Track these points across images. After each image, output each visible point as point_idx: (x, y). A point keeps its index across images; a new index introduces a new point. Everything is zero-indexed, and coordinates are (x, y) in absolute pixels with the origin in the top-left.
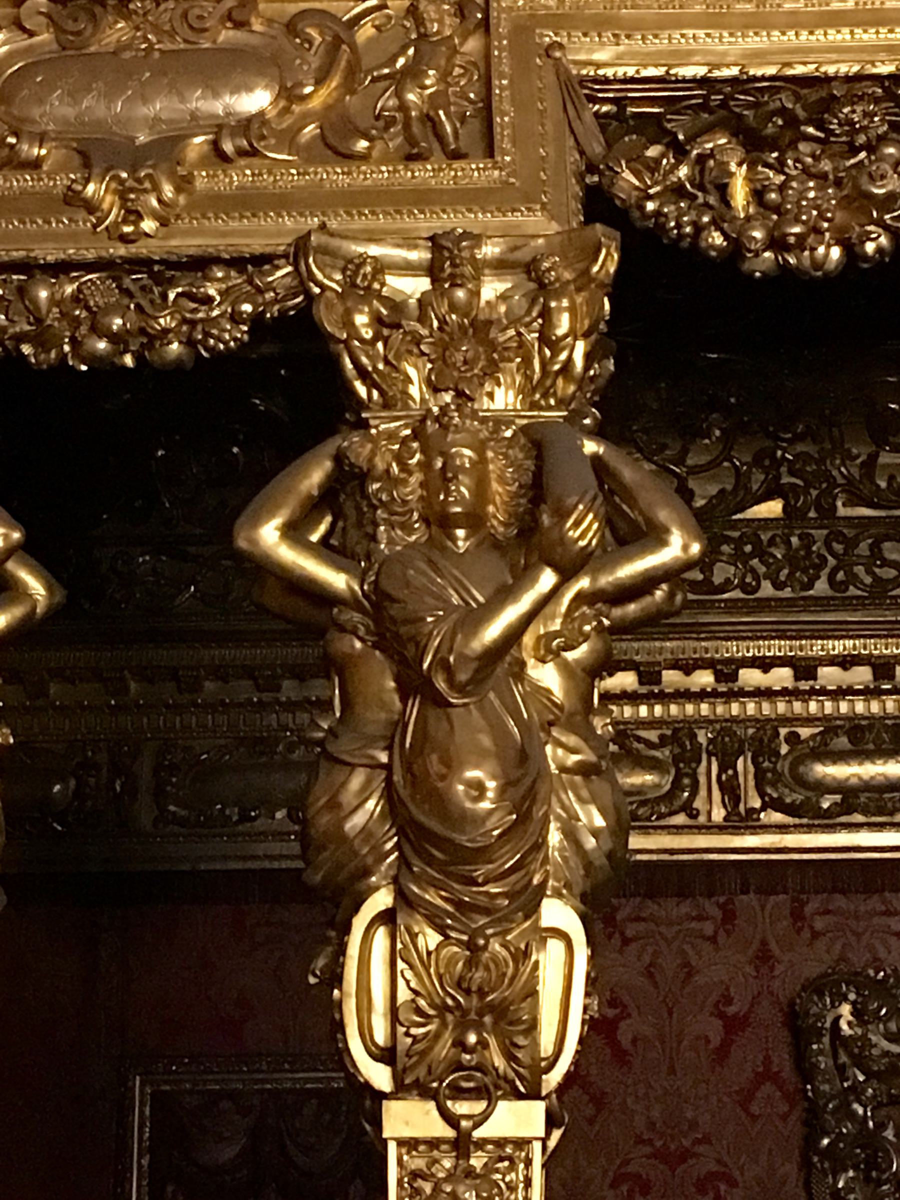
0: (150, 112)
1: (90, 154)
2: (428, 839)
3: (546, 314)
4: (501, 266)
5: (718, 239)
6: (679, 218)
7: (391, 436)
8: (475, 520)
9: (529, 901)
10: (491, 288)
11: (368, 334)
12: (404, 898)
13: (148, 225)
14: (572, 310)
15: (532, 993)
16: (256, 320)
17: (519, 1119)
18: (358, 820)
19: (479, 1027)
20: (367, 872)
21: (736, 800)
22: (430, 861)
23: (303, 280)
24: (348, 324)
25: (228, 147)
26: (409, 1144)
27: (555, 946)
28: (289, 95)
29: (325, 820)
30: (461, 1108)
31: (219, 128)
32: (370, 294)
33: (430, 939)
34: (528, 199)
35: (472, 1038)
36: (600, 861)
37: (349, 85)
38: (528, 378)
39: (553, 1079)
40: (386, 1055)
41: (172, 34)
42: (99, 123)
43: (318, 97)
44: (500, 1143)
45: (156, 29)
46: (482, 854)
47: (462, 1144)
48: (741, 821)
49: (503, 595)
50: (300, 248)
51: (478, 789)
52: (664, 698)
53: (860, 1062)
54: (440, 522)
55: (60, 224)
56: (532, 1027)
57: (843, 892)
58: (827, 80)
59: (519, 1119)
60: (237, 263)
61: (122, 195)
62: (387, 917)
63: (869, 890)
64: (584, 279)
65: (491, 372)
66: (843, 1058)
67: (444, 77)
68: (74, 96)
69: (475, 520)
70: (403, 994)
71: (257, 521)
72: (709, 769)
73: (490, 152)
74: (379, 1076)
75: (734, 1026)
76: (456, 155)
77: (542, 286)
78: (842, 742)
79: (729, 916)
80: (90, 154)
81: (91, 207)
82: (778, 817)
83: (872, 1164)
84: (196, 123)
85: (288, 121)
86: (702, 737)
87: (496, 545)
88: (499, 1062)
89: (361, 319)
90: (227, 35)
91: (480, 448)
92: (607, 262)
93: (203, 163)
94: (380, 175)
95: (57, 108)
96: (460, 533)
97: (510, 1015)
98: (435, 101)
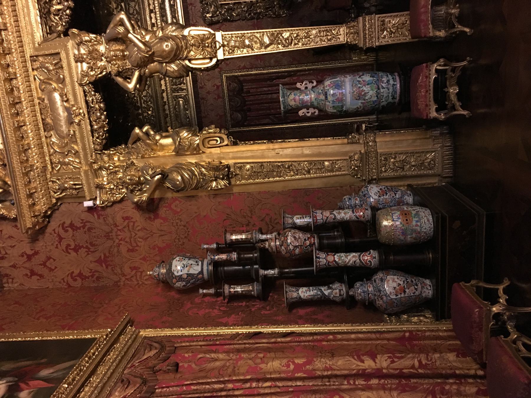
1: (70, 122)
3: (86, 41)
4: (79, 50)
5: (68, 12)
6: (65, 19)
7: (111, 67)
9: (184, 37)
10: (83, 51)
11: (94, 72)
12: (186, 58)
13: (81, 111)
14: (84, 37)
15: (199, 35)
16: (95, 92)
17: (219, 35)
18: (176, 68)
19: (205, 44)
20: (183, 65)
22: (180, 54)
23: (86, 84)
24: (93, 76)
25: (65, 99)
26: (224, 54)
28: (55, 90)
29: (176, 74)
30: (218, 47)
31: (63, 101)
32: (87, 72)
33: (192, 53)
34: (66, 46)
35: (207, 45)
37: (51, 79)
38: (97, 44)
39: (212, 32)
40: (211, 59)
41: (47, 111)
42: (66, 122)
43: (54, 85)
44: (223, 39)
45: (47, 114)
46: (177, 45)
47: (223, 46)
49: (135, 45)
50: (81, 85)
51: (167, 46)
53: (216, 13)
54: (124, 57)
56: (204, 35)
57: (189, 17)
59: (219, 35)
60: (86, 96)
61: (77, 116)
62: (190, 61)
64: (79, 35)
65: (97, 50)
66: (215, 15)
67: (47, 63)
69: (123, 51)
70: (201, 57)
71: (128, 88)
73: (58, 54)
74: (214, 61)
76: (60, 59)
77: (81, 43)
78: (164, 18)
81: (80, 121)
83: (231, 9)
84: (63, 105)
85: (59, 89)
87: (127, 48)
88: (210, 40)
89: (92, 73)
90: (46, 101)
91: (110, 51)
92: (75, 31)
93: (69, 103)
94: (66, 73)
95: (64, 128)
96: (125, 53)
97: (203, 39)
98: (52, 64)
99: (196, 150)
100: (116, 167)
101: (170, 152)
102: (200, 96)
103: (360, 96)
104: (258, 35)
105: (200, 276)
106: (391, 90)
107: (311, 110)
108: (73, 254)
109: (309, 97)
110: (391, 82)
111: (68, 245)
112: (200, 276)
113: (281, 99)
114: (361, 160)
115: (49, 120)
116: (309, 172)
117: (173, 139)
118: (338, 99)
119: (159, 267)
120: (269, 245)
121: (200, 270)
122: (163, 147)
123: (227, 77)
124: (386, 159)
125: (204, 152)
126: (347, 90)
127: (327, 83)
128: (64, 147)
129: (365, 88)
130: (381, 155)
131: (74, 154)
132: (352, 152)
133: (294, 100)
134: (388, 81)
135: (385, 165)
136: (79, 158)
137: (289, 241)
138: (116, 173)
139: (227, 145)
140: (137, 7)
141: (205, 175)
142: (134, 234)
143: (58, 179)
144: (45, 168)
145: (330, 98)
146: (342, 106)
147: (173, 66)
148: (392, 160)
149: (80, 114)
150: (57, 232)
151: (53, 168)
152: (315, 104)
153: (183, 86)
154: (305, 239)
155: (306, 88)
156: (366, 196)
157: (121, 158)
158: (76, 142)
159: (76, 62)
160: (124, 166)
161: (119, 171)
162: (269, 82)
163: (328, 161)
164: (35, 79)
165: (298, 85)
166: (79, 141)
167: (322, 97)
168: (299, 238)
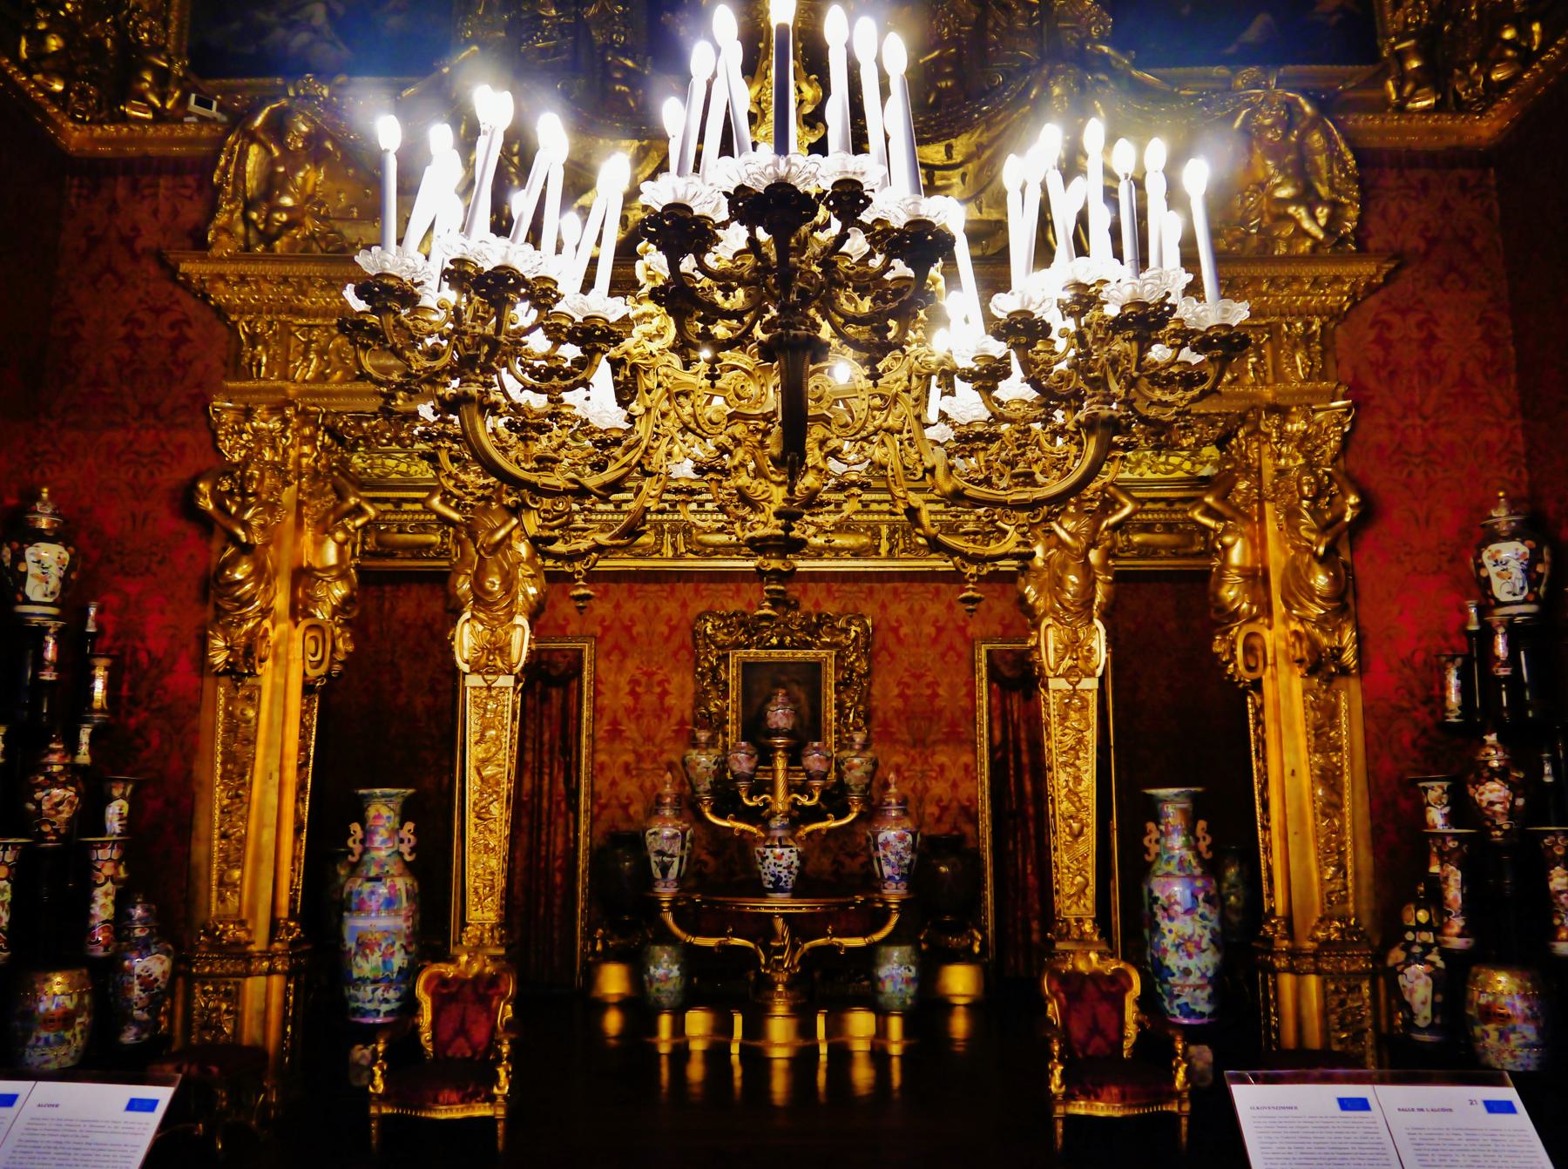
2: (482, 599)
12: (473, 616)
15: (509, 644)
21: (675, 549)
30: (488, 677)
33: (480, 628)
39: (517, 670)
40: (467, 662)
47: (489, 688)
48: (678, 556)
53: (714, 643)
59: (507, 681)
63: (722, 582)
72: (668, 538)
74: (465, 668)
75: (673, 629)
79: (672, 591)
82: (690, 555)
86: (666, 526)
88: (500, 664)
99: (298, 611)
100: (285, 451)
101: (308, 556)
103: (364, 946)
104: (500, 756)
105: (20, 598)
106: (369, 1006)
107: (357, 848)
108: (122, 331)
109: (382, 849)
110: (384, 1008)
111: (141, 325)
112: (20, 598)
113: (378, 791)
114: (237, 943)
116: (224, 836)
117: (331, 568)
118: (362, 902)
119: (53, 514)
120: (54, 751)
121: (33, 598)
122: (319, 544)
123: (581, 651)
124: (227, 994)
125: (296, 624)
126: (379, 922)
127: (402, 884)
128: (338, 355)
129: (378, 954)
130: (237, 984)
131: (322, 373)
132: (255, 925)
133: (378, 816)
134: (386, 1001)
135: (216, 991)
136: (316, 380)
137: (55, 791)
138: (274, 448)
139: (305, 674)
141: (239, 626)
142: (145, 461)
143: (275, 333)
144: (300, 312)
145: (367, 886)
146: (349, 910)
147: (467, 586)
148: (224, 1006)
150: (175, 307)
151: (301, 326)
152: (366, 857)
154: (53, 824)
155: (402, 841)
156: (144, 948)
157: (304, 461)
158: (343, 381)
160: (285, 465)
161: (276, 453)
162: (558, 744)
163: (241, 878)
165: (410, 826)
166: (346, 386)
167: (373, 872)
168: (59, 812)
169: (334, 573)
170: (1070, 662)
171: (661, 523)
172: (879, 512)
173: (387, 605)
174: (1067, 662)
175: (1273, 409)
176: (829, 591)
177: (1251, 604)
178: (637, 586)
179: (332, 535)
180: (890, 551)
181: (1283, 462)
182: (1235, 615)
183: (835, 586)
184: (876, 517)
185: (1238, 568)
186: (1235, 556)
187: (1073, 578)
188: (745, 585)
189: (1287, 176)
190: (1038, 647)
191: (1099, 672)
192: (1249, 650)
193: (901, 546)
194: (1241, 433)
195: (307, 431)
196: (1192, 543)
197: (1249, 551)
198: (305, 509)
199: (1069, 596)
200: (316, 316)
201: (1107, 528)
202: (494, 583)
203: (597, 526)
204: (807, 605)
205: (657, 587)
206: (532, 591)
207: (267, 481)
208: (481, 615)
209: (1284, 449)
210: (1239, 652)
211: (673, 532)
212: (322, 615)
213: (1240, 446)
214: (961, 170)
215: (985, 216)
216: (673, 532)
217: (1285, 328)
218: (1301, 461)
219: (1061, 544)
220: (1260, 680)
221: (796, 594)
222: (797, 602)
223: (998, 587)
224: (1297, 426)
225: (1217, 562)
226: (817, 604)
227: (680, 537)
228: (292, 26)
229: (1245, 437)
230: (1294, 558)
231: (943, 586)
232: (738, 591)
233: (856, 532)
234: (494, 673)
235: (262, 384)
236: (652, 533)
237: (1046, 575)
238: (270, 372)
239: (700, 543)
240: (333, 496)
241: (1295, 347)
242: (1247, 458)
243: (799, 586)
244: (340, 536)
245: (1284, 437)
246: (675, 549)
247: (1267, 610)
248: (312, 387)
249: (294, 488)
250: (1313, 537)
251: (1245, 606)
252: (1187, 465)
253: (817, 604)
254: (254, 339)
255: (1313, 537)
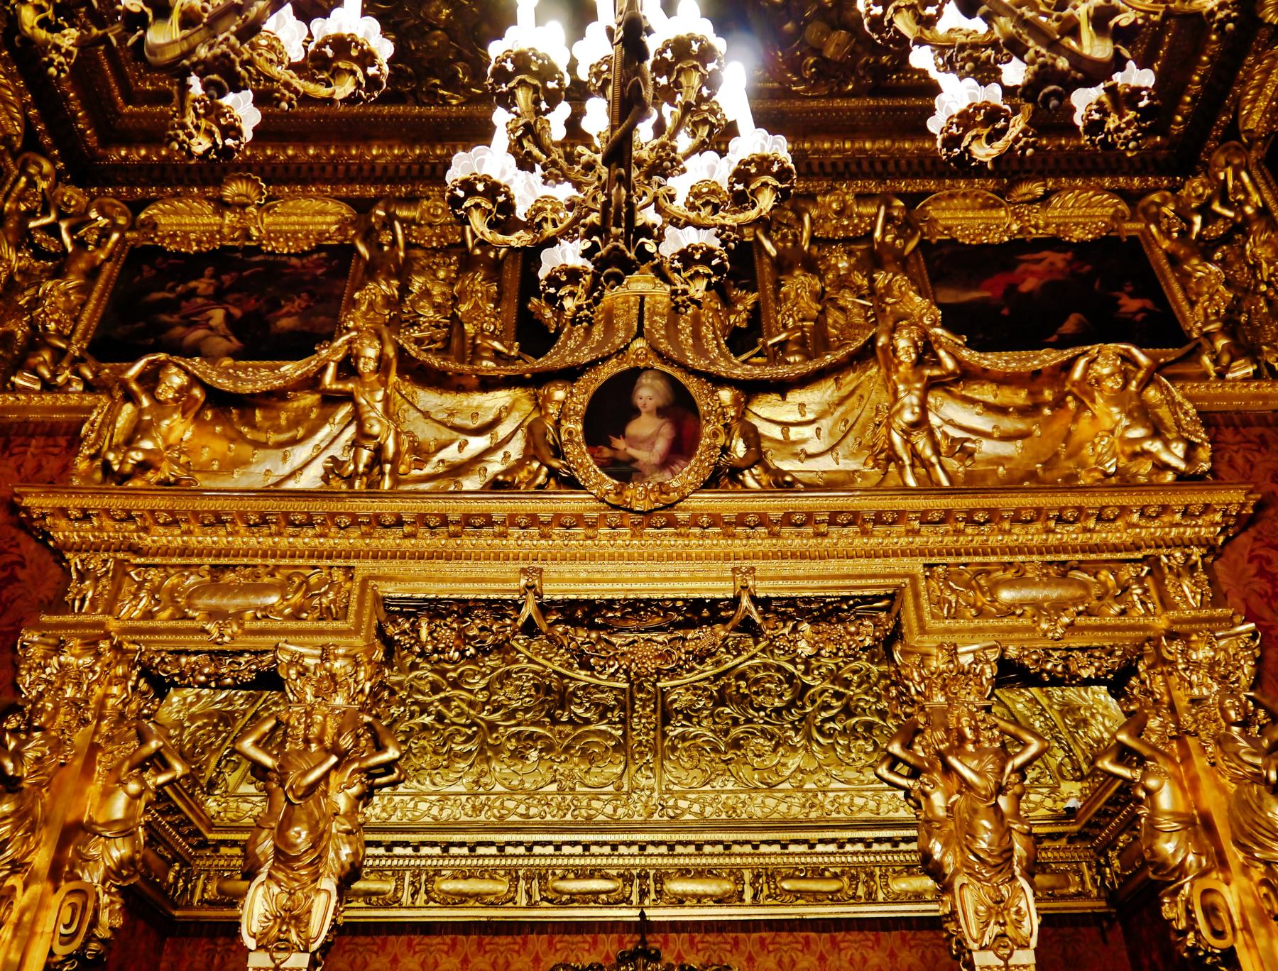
0: (231, 603)
1: (213, 615)
2: (283, 857)
8: (320, 741)
12: (270, 876)
13: (226, 639)
21: (530, 897)
23: (275, 659)
27: (323, 896)
31: (258, 608)
33: (276, 890)
36: (348, 867)
40: (254, 936)
46: (297, 859)
48: (531, 905)
52: (506, 856)
54: (307, 741)
55: (198, 638)
58: (467, 601)
60: (256, 653)
64: (370, 662)
68: (211, 597)
69: (320, 741)
74: (251, 943)
79: (525, 943)
80: (213, 615)
82: (545, 904)
86: (521, 873)
88: (293, 937)
90: (267, 580)
91: (325, 717)
94: (308, 625)
95: (205, 602)
101: (89, 807)
102: (393, 938)
115: (230, 577)
117: (116, 822)
122: (107, 794)
138: (78, 685)
140: (601, 818)
144: (137, 551)
149: (222, 635)
151: (138, 566)
153: (422, 897)
157: (110, 702)
158: (172, 618)
159: (324, 648)
164: (314, 567)
166: (173, 624)
169: (117, 828)
170: (997, 929)
171: (517, 868)
172: (741, 855)
173: (216, 961)
174: (993, 930)
175: (1171, 636)
176: (692, 942)
177: (1199, 854)
178: (487, 939)
179: (123, 784)
180: (755, 897)
181: (1196, 691)
182: (1181, 869)
183: (698, 937)
184: (738, 860)
185: (1171, 813)
186: (1165, 800)
187: (986, 823)
188: (603, 936)
189: (1133, 419)
190: (953, 913)
191: (1034, 942)
192: (1211, 911)
193: (766, 892)
194: (1141, 667)
195: (120, 670)
196: (1068, 884)
197: (1179, 794)
198: (99, 756)
199: (984, 846)
200: (154, 555)
201: (1013, 771)
202: (300, 835)
203: (448, 873)
204: (668, 958)
205: (509, 939)
206: (346, 851)
207: (61, 719)
208: (280, 875)
209: (1194, 678)
210: (1199, 915)
211: (529, 879)
212: (92, 877)
213: (1143, 682)
214: (815, 426)
215: (841, 467)
216: (529, 879)
217: (1165, 560)
218: (1216, 687)
219: (966, 786)
220: (1232, 949)
221: (657, 945)
222: (658, 952)
223: (870, 935)
224: (1202, 653)
225: (1144, 811)
226: (679, 957)
227: (535, 884)
228: (192, 325)
229: (1146, 671)
230: (1237, 791)
231: (812, 935)
232: (595, 943)
233: (718, 876)
234: (286, 949)
235: (82, 618)
236: (506, 880)
237: (952, 826)
238: (93, 606)
239: (555, 890)
240: (135, 743)
241: (1178, 575)
242: (1152, 693)
243: (659, 937)
244: (134, 787)
245: (1194, 666)
246: (530, 897)
247: (1223, 864)
248: (137, 624)
249: (91, 728)
250: (1259, 761)
251: (1191, 858)
252: (1049, 803)
253: (679, 957)
254: (82, 577)
255: (1259, 761)
